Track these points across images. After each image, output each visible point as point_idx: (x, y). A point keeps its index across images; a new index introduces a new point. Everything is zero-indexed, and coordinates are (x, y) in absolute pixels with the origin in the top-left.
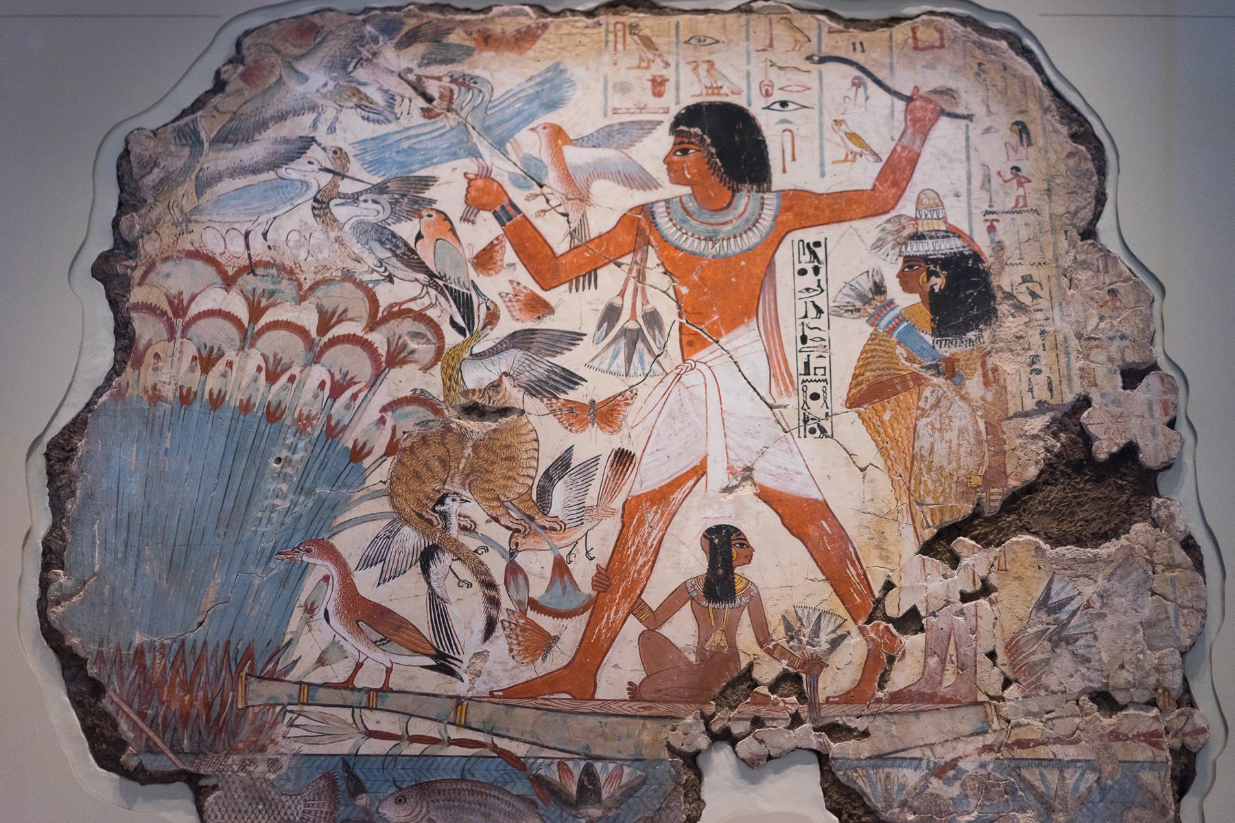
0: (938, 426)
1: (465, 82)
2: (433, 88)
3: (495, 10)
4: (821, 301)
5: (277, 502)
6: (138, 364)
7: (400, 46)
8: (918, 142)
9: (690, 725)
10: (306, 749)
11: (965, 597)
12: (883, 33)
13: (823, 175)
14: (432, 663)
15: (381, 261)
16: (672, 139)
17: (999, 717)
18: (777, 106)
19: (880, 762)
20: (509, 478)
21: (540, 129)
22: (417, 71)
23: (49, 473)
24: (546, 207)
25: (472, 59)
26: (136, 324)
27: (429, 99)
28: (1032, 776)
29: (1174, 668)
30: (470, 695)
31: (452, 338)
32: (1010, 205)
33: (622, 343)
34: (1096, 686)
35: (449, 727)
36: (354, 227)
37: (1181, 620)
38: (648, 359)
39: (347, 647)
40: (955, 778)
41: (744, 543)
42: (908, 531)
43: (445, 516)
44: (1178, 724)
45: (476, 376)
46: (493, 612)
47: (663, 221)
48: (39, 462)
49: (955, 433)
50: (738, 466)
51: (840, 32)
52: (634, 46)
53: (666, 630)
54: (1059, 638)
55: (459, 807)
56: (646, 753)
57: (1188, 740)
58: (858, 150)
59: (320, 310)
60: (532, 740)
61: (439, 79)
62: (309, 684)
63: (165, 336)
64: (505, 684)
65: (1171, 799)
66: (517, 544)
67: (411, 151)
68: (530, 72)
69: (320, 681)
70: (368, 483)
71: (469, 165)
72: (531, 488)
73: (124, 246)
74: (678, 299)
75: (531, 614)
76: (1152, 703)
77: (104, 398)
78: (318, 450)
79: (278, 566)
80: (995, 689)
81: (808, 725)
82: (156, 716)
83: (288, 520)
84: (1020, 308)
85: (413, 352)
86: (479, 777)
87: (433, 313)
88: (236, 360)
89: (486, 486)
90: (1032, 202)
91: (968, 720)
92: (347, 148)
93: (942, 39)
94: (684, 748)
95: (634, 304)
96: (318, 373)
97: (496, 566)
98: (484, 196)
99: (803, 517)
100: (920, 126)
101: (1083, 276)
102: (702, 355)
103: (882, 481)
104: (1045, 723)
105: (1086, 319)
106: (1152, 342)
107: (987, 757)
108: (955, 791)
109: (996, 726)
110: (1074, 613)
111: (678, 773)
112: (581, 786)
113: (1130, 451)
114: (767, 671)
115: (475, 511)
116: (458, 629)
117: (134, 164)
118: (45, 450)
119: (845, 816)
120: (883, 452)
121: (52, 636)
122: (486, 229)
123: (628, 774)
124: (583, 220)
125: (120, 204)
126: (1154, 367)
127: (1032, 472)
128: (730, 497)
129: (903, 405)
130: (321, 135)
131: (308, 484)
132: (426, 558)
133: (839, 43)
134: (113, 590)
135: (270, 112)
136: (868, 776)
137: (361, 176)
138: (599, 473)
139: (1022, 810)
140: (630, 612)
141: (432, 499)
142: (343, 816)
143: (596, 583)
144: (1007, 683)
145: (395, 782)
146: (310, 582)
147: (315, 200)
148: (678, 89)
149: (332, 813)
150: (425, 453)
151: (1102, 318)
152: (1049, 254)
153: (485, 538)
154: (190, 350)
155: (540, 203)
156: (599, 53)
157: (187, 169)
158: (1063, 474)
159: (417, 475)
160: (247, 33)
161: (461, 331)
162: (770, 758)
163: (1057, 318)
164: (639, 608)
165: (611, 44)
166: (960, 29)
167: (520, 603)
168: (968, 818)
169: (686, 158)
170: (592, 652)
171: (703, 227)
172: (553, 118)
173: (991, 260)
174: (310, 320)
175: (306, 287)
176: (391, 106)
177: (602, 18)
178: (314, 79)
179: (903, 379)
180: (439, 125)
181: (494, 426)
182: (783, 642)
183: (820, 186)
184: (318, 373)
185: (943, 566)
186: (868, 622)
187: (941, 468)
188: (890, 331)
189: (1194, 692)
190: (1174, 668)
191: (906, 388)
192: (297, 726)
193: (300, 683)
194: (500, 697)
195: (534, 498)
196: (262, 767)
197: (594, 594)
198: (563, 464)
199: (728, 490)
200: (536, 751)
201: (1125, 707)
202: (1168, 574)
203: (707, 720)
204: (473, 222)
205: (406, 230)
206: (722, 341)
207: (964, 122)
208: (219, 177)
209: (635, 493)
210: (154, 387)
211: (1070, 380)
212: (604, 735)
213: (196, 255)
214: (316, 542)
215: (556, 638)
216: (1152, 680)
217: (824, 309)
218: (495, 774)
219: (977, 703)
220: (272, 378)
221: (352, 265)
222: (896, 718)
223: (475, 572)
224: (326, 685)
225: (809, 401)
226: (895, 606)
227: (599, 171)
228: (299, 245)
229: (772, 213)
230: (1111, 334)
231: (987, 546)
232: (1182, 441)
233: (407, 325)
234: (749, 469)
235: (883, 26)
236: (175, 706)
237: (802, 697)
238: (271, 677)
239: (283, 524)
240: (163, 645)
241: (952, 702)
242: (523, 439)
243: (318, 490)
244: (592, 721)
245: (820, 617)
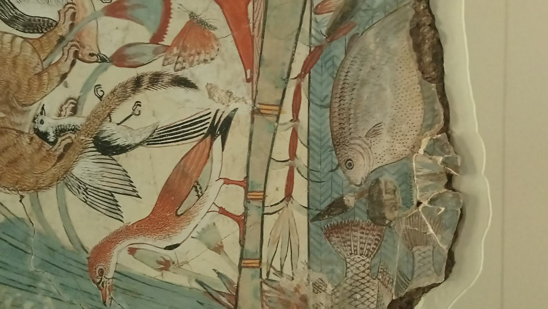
10: (304, 256)
14: (219, 140)
20: (14, 63)
30: (250, 102)
35: (281, 121)
39: (203, 224)
43: (60, 131)
46: (166, 79)
60: (293, 40)
62: (241, 259)
64: (240, 67)
66: (92, 55)
69: (238, 248)
72: (25, 39)
75: (168, 41)
83: (66, 297)
89: (25, 87)
97: (115, 77)
115: (54, 99)
131: (25, 280)
132: (107, 148)
141: (41, 146)
142: (365, 217)
145: (332, 171)
146: (138, 268)
149: (362, 228)
159: (13, 162)
167: (156, 52)
192: (282, 267)
193: (240, 268)
194: (252, 72)
195: (38, 36)
196: (322, 298)
215: (192, 15)
218: (326, 75)
223: (124, 98)
224: (242, 242)
238: (235, 298)
239: (71, 303)
243: (32, 268)
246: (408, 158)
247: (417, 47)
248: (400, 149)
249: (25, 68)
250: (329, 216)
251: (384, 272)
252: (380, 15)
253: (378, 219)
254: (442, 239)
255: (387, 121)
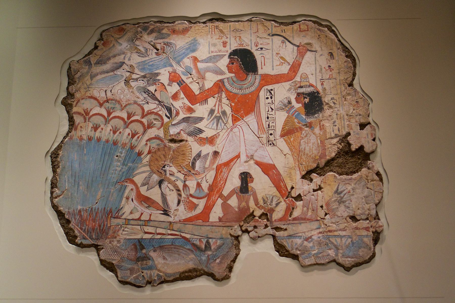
0: (306, 142)
1: (168, 44)
2: (159, 47)
3: (176, 22)
4: (273, 106)
5: (117, 168)
6: (76, 129)
7: (148, 34)
8: (301, 59)
9: (236, 228)
10: (128, 237)
11: (314, 191)
12: (290, 27)
13: (273, 69)
14: (163, 212)
15: (145, 98)
16: (229, 60)
17: (324, 224)
18: (260, 49)
19: (290, 237)
21: (190, 58)
22: (154, 41)
23: (51, 161)
24: (193, 81)
25: (170, 37)
26: (75, 118)
27: (158, 50)
28: (333, 240)
29: (373, 209)
31: (166, 120)
32: (328, 77)
33: (215, 120)
34: (351, 214)
36: (137, 88)
37: (376, 195)
38: (223, 124)
39: (138, 209)
40: (311, 241)
41: (251, 177)
42: (298, 172)
43: (165, 171)
44: (374, 225)
45: (173, 131)
46: (180, 198)
47: (226, 84)
48: (49, 159)
49: (311, 144)
50: (249, 155)
51: (278, 27)
52: (217, 33)
53: (229, 202)
54: (341, 202)
55: (172, 253)
56: (224, 236)
57: (377, 229)
58: (283, 62)
59: (128, 112)
61: (160, 44)
63: (84, 121)
64: (184, 218)
65: (372, 246)
67: (152, 65)
68: (187, 41)
69: (131, 218)
70: (143, 162)
71: (170, 69)
73: (70, 95)
74: (231, 106)
75: (190, 198)
76: (367, 219)
77: (67, 139)
78: (128, 153)
79: (118, 186)
80: (323, 216)
81: (270, 228)
82: (85, 229)
83: (121, 173)
84: (331, 107)
85: (155, 124)
86: (177, 244)
87: (160, 113)
88: (104, 128)
89: (177, 162)
90: (334, 76)
91: (315, 225)
92: (134, 65)
93: (308, 28)
94: (235, 235)
95: (218, 109)
96: (128, 131)
97: (180, 185)
98: (174, 78)
99: (268, 169)
100: (301, 54)
101: (349, 97)
102: (238, 123)
103: (291, 159)
104: (337, 225)
105: (349, 110)
106: (369, 116)
107: (320, 235)
108: (311, 244)
109: (323, 226)
110: (345, 194)
111: (233, 242)
112: (206, 246)
113: (362, 147)
114: (258, 213)
116: (170, 203)
117: (72, 71)
118: (50, 155)
119: (280, 253)
120: (291, 150)
121: (55, 207)
122: (175, 88)
123: (219, 242)
124: (203, 85)
125: (69, 83)
126: (369, 123)
127: (333, 155)
128: (247, 164)
129: (297, 136)
130: (126, 61)
131: (126, 163)
133: (278, 30)
134: (72, 194)
135: (111, 55)
136: (287, 241)
137: (139, 73)
138: (209, 158)
139: (330, 249)
140: (219, 197)
142: (139, 256)
143: (209, 189)
144: (326, 214)
146: (127, 191)
147: (125, 80)
148: (230, 45)
150: (159, 153)
151: (354, 110)
152: (339, 91)
153: (177, 177)
154: (91, 125)
155: (191, 80)
156: (207, 35)
157: (88, 73)
158: (343, 155)
159: (157, 160)
160: (104, 31)
161: (169, 118)
162: (259, 237)
163: (341, 110)
164: (221, 196)
165: (211, 32)
166: (313, 25)
167: (187, 195)
168: (315, 252)
170: (208, 209)
171: (238, 86)
172: (194, 54)
173: (322, 93)
174: (125, 116)
175: (123, 106)
176: (146, 52)
177: (208, 24)
178: (124, 45)
179: (297, 129)
180: (161, 57)
181: (179, 145)
182: (262, 204)
183: (272, 73)
184: (128, 131)
185: (308, 182)
186: (286, 198)
187: (307, 154)
188: (294, 114)
189: (379, 216)
190: (373, 209)
191: (298, 131)
193: (125, 219)
197: (208, 192)
198: (199, 155)
199: (246, 162)
200: (193, 236)
201: (359, 220)
202: (372, 183)
203: (241, 227)
204: (171, 86)
205: (152, 89)
206: (244, 119)
207: (314, 53)
208: (97, 75)
209: (220, 163)
210: (81, 136)
211: (344, 128)
212: (212, 232)
213: (91, 97)
214: (129, 179)
215: (198, 205)
216: (367, 213)
217: (274, 109)
218: (181, 243)
219: (317, 220)
220: (114, 132)
221: (137, 99)
222: (294, 225)
224: (133, 219)
225: (270, 136)
226: (294, 193)
227: (208, 70)
228: (121, 94)
229: (258, 81)
230: (356, 114)
231: (321, 176)
232: (377, 145)
233: (153, 116)
234: (252, 156)
235: (291, 24)
236: (90, 226)
237: (268, 220)
238: (117, 218)
240: (86, 209)
241: (310, 220)
242: (187, 148)
244: (208, 228)
245: (273, 197)
246: (156, 269)
247: (190, 271)
248: (159, 266)
249: (182, 162)
250: (139, 245)
251: (123, 262)
252: (199, 259)
253: (138, 260)
254: (132, 279)
255: (168, 262)
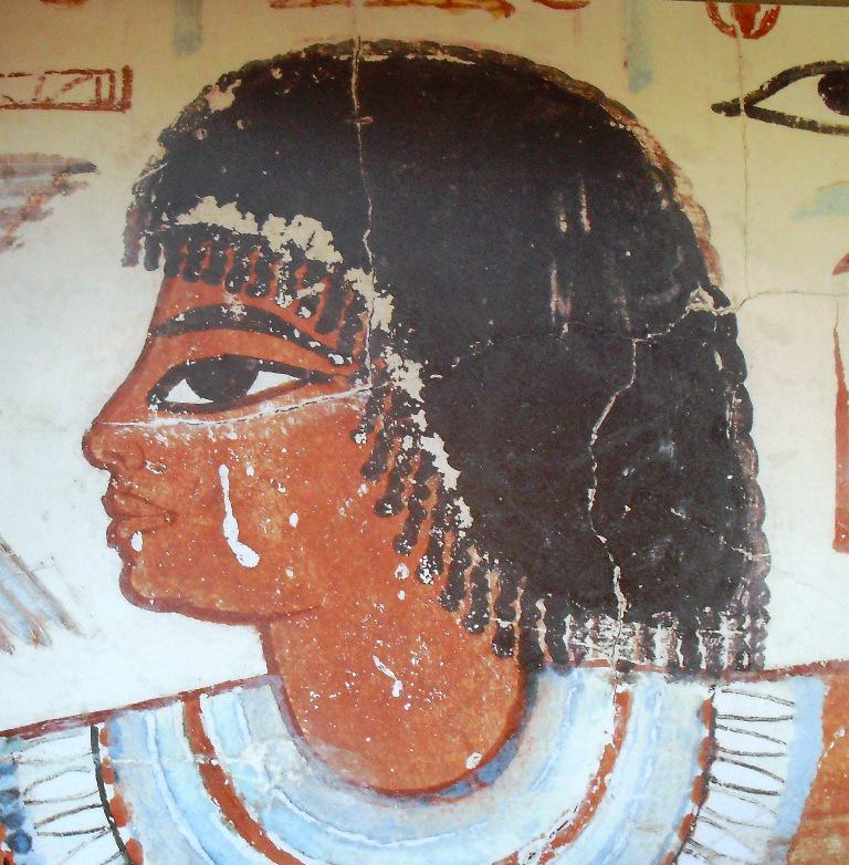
16: (141, 290)
169: (230, 426)
